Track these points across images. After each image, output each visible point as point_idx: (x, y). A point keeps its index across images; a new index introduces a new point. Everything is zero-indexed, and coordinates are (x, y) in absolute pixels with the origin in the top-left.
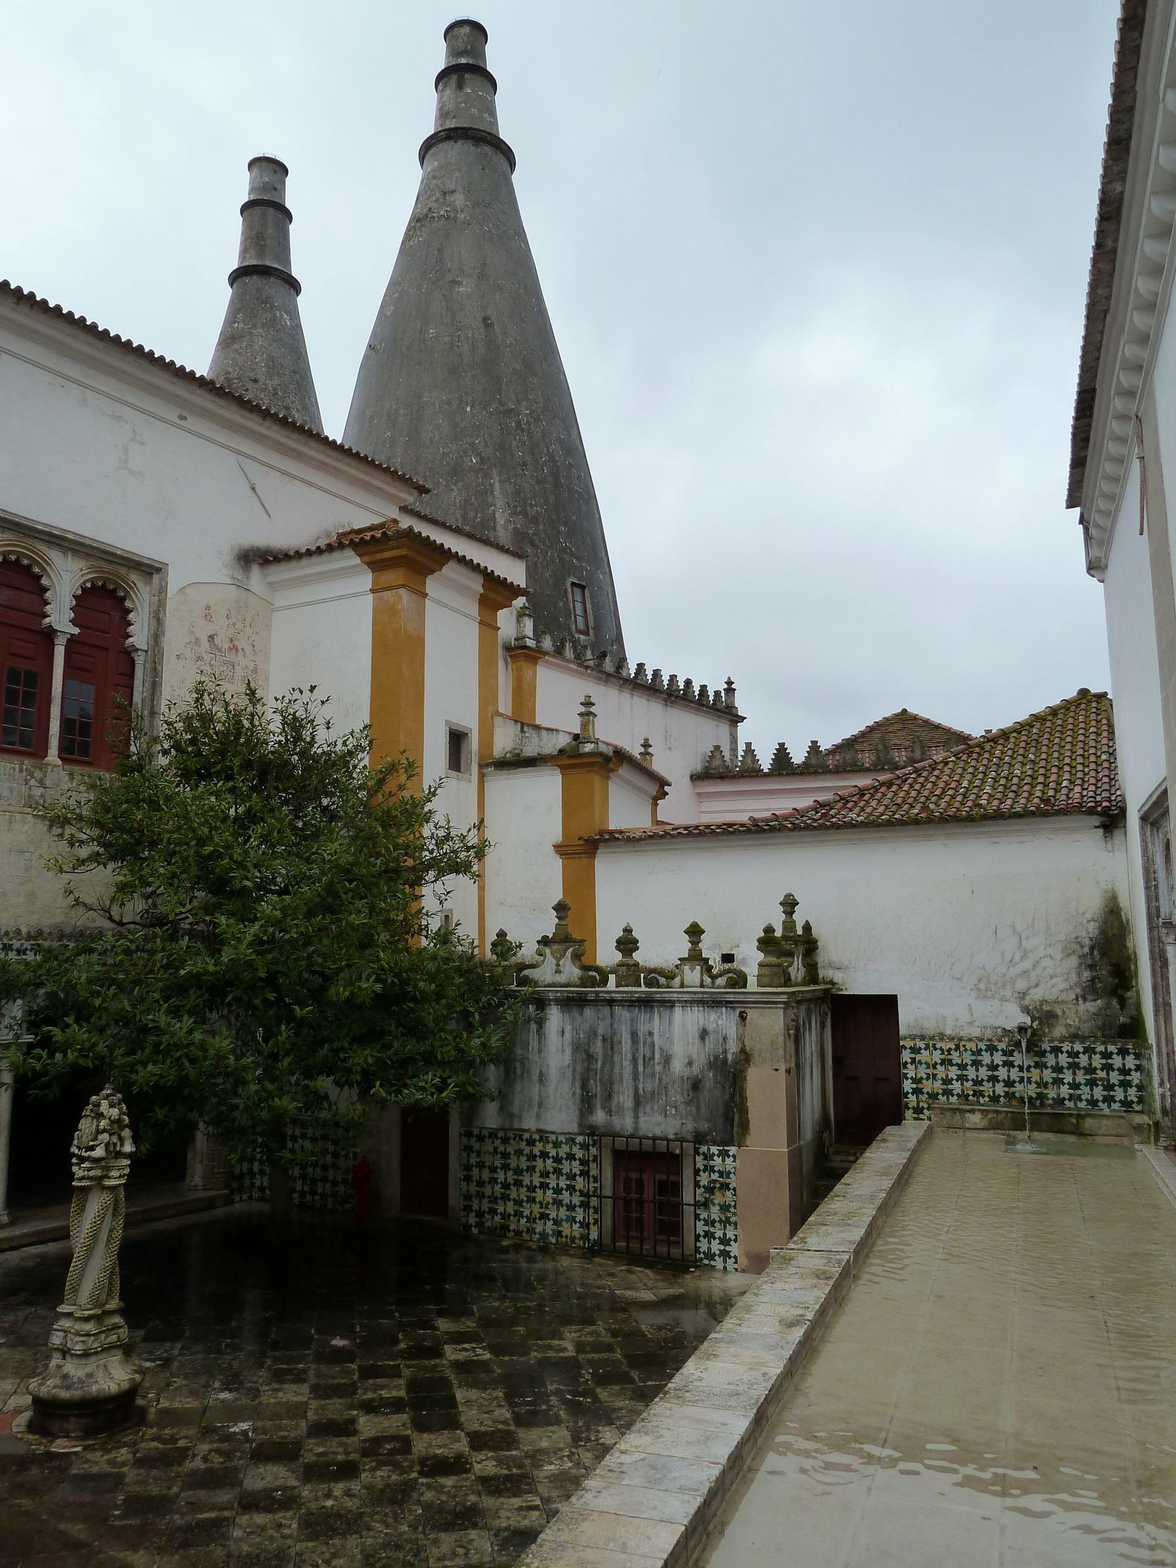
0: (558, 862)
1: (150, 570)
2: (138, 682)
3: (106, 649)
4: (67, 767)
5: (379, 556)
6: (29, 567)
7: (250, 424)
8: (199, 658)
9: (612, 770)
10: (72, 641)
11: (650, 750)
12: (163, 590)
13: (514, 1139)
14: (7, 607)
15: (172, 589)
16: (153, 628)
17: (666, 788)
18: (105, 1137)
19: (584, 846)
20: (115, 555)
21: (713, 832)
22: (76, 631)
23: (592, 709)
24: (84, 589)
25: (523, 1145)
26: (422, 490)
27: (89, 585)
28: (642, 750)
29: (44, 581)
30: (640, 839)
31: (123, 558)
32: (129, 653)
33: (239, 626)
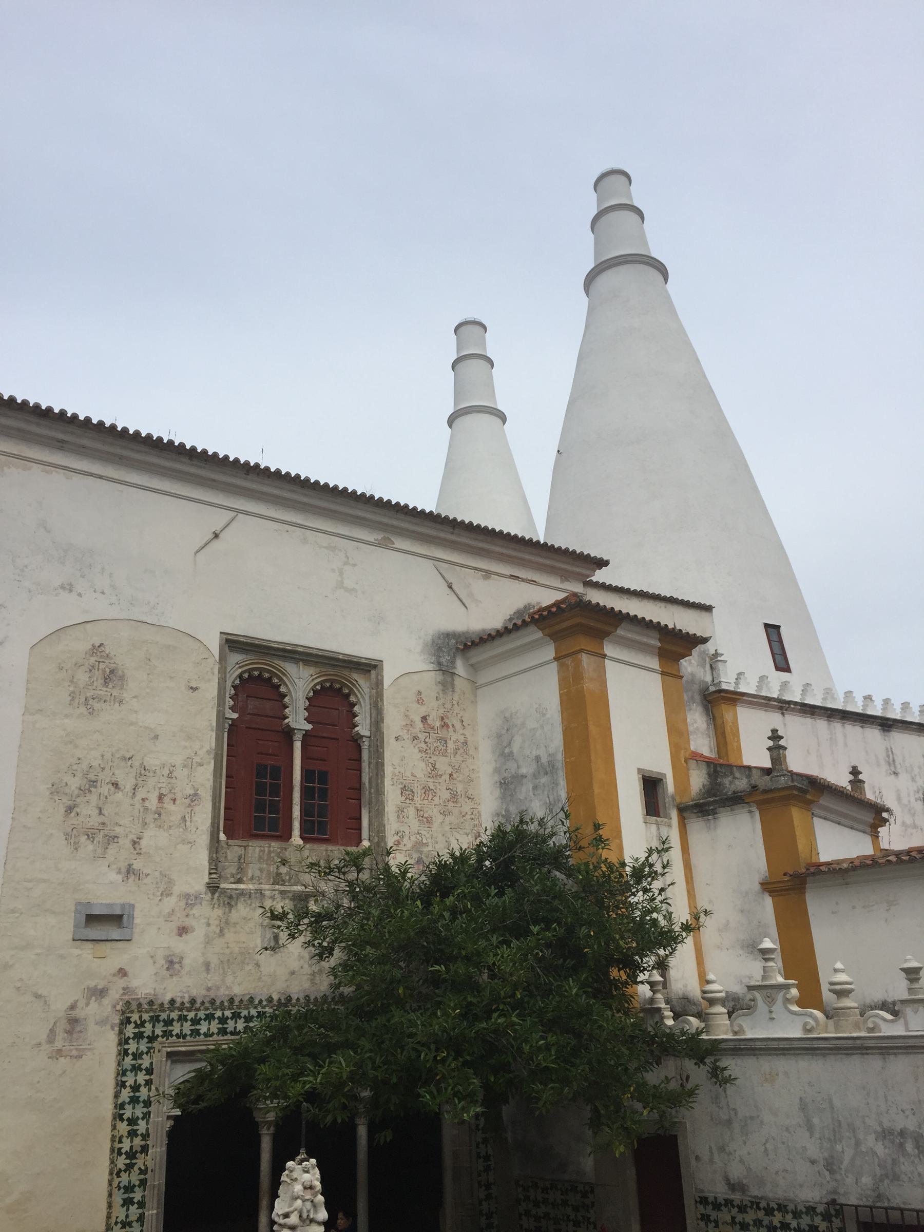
0: (768, 901)
1: (370, 667)
2: (365, 765)
3: (337, 739)
4: (308, 846)
5: (557, 627)
6: (270, 679)
7: (442, 535)
8: (415, 738)
9: (810, 802)
10: (307, 735)
11: (861, 777)
12: (379, 684)
13: (751, 1208)
14: (255, 715)
15: (387, 682)
16: (374, 715)
17: (885, 815)
18: (299, 1202)
19: (792, 884)
20: (338, 660)
21: (913, 860)
22: (309, 727)
23: (782, 742)
24: (315, 692)
25: (761, 1214)
26: (602, 563)
27: (319, 687)
28: (851, 777)
29: (283, 689)
30: (846, 871)
31: (344, 661)
32: (356, 740)
33: (448, 706)
